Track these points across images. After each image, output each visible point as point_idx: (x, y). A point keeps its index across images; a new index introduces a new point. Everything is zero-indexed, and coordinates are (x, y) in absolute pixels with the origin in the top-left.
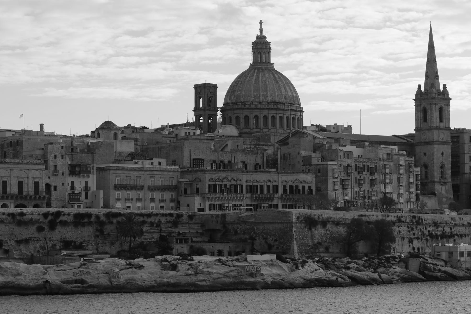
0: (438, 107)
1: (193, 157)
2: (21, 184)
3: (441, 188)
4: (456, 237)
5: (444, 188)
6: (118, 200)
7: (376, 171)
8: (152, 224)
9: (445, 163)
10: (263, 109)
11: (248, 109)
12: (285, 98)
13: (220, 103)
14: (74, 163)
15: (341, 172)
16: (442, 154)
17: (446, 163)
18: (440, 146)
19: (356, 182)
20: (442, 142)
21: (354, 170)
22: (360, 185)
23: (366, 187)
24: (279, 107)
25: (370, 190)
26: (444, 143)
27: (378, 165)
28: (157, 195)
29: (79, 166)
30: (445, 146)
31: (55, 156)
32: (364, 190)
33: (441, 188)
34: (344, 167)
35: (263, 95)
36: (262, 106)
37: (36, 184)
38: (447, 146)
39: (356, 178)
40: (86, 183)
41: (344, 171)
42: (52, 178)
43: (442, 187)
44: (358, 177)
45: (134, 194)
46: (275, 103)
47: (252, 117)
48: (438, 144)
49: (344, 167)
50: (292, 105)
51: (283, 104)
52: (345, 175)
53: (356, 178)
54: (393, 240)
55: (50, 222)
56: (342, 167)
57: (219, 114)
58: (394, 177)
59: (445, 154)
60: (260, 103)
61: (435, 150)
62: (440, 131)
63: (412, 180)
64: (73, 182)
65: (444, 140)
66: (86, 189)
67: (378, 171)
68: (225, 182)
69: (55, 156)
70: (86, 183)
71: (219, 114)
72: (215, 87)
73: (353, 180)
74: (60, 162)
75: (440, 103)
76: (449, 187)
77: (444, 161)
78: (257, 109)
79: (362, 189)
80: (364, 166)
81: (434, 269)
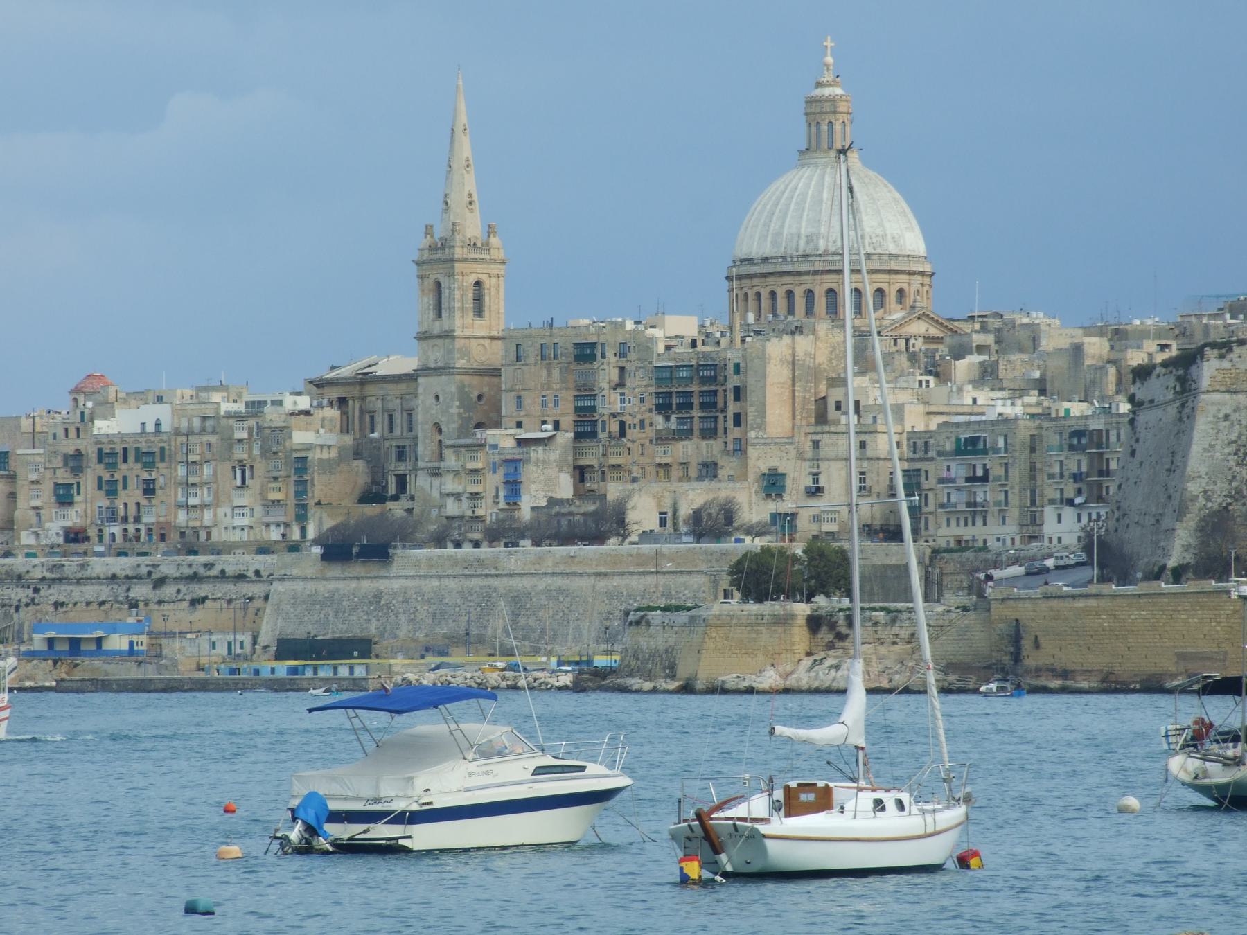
7: (162, 460)
9: (443, 420)
12: (775, 243)
15: (55, 469)
16: (437, 397)
18: (431, 379)
19: (100, 488)
20: (435, 369)
21: (95, 460)
22: (112, 492)
23: (131, 496)
25: (144, 502)
27: (169, 445)
34: (66, 458)
38: (447, 377)
41: (66, 464)
44: (107, 477)
46: (751, 261)
47: (781, 293)
52: (68, 475)
53: (100, 478)
56: (60, 458)
61: (420, 390)
62: (431, 342)
65: (439, 364)
67: (167, 459)
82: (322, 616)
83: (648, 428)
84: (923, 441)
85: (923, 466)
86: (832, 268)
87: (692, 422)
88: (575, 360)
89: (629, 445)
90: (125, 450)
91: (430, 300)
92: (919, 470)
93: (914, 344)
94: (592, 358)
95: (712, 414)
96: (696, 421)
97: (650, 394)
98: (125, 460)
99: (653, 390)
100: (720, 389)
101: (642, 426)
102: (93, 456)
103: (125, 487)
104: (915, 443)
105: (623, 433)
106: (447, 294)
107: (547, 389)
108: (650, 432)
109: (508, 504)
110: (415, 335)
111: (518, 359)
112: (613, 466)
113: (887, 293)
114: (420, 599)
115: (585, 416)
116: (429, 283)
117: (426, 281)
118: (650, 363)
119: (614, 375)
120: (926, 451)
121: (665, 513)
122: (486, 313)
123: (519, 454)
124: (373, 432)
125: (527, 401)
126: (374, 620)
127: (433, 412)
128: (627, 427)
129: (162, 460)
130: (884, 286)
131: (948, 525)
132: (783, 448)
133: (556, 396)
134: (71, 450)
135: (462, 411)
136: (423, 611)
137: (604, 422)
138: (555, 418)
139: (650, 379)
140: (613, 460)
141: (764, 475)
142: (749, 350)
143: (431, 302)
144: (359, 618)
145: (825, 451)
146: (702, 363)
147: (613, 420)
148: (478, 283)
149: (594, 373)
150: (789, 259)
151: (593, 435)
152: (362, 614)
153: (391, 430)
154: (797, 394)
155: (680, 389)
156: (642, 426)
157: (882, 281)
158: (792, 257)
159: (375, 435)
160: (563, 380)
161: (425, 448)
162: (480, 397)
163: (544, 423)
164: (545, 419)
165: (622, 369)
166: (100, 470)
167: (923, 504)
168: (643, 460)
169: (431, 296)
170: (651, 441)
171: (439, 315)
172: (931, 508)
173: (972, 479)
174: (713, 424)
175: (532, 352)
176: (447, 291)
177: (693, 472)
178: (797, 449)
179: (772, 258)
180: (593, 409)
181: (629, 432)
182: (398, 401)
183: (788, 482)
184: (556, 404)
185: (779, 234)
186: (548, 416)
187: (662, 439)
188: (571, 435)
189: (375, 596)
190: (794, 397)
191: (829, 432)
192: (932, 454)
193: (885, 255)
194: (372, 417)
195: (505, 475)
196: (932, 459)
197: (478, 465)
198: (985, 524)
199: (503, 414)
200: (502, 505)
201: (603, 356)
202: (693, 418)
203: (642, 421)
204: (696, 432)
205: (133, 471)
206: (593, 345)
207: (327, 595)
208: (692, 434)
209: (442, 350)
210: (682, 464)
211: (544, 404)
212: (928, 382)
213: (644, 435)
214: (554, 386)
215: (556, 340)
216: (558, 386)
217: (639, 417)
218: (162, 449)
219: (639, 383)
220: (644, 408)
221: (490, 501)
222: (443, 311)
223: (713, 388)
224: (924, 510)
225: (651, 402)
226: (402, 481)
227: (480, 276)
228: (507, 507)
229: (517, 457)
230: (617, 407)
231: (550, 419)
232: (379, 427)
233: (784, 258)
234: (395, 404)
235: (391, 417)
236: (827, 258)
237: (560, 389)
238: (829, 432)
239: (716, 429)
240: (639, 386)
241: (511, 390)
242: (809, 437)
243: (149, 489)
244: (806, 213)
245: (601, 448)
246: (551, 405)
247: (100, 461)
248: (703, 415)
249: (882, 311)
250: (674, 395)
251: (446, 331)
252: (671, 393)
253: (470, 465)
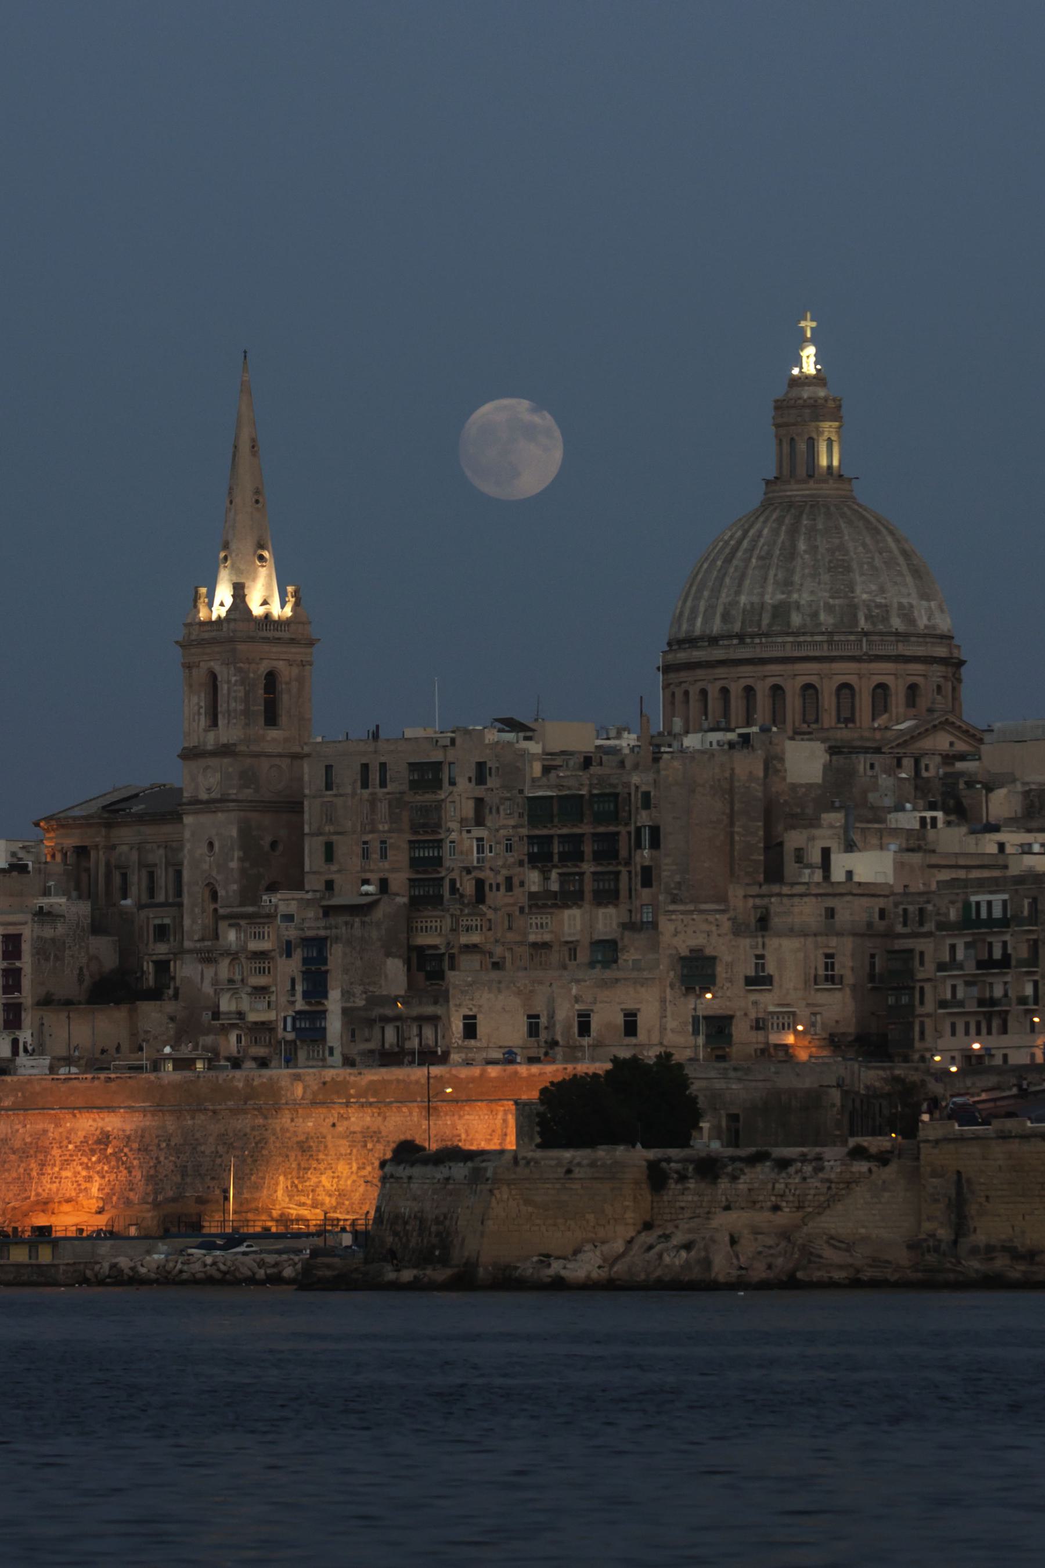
3: (202, 971)
5: (209, 972)
12: (726, 617)
16: (211, 845)
17: (219, 878)
18: (205, 819)
30: (220, 814)
33: (202, 971)
43: (205, 970)
48: (196, 813)
50: (748, 640)
51: (713, 641)
61: (187, 835)
65: (213, 795)
75: (206, 658)
77: (214, 873)
82: (21, 1170)
83: (517, 890)
84: (917, 907)
86: (811, 654)
87: (581, 881)
88: (411, 788)
89: (490, 914)
91: (199, 700)
92: (911, 951)
93: (927, 769)
94: (436, 784)
95: (611, 868)
96: (588, 879)
97: (521, 838)
99: (524, 831)
100: (621, 829)
101: (509, 888)
104: (905, 910)
105: (480, 896)
106: (225, 691)
107: (372, 832)
108: (519, 896)
109: (309, 1003)
110: (179, 751)
111: (329, 786)
112: (467, 946)
113: (893, 691)
114: (164, 1145)
115: (425, 872)
116: (200, 675)
117: (195, 671)
118: (521, 791)
119: (468, 809)
120: (921, 923)
121: (537, 1017)
122: (283, 720)
123: (325, 928)
124: (125, 898)
125: (340, 851)
126: (97, 1178)
127: (206, 867)
128: (487, 888)
130: (889, 680)
131: (953, 1033)
132: (711, 918)
133: (383, 842)
135: (247, 865)
137: (453, 882)
138: (382, 875)
139: (521, 815)
140: (464, 939)
141: (682, 959)
142: (663, 773)
143: (202, 704)
144: (76, 1174)
145: (776, 921)
146: (595, 792)
147: (467, 878)
148: (271, 677)
149: (439, 806)
150: (748, 640)
151: (437, 901)
152: (80, 1168)
153: (151, 892)
154: (737, 838)
155: (565, 831)
156: (509, 888)
157: (883, 672)
158: (752, 636)
159: (128, 902)
161: (194, 922)
162: (274, 845)
163: (366, 882)
164: (368, 876)
165: (479, 802)
167: (917, 1002)
168: (510, 936)
169: (203, 695)
170: (522, 910)
171: (215, 724)
172: (929, 1007)
173: (986, 964)
174: (612, 884)
175: (347, 777)
176: (225, 686)
177: (583, 956)
178: (733, 920)
179: (723, 637)
180: (438, 861)
181: (490, 896)
182: (161, 851)
183: (720, 969)
184: (384, 855)
185: (734, 603)
186: (372, 871)
187: (541, 902)
188: (403, 900)
189: (99, 1142)
190: (732, 843)
191: (779, 895)
192: (929, 926)
193: (890, 634)
194: (124, 876)
195: (306, 961)
196: (929, 934)
197: (265, 945)
199: (307, 868)
201: (453, 783)
202: (582, 874)
203: (509, 880)
204: (588, 895)
206: (437, 766)
207: (28, 1140)
208: (582, 899)
209: (218, 775)
210: (567, 942)
211: (366, 855)
212: (934, 820)
213: (511, 900)
214: (381, 827)
215: (383, 759)
216: (386, 828)
217: (505, 872)
220: (511, 860)
221: (283, 1000)
222: (220, 716)
223: (612, 829)
224: (919, 1010)
225: (522, 850)
226: (162, 967)
227: (275, 663)
228: (306, 1008)
229: (322, 933)
231: (374, 877)
232: (134, 890)
233: (741, 637)
234: (157, 856)
235: (151, 875)
236: (801, 639)
237: (389, 831)
238: (779, 895)
239: (617, 892)
240: (505, 827)
241: (319, 833)
242: (751, 902)
244: (772, 573)
245: (449, 920)
246: (376, 856)
248: (599, 869)
249: (885, 716)
250: (556, 841)
251: (224, 745)
252: (551, 837)
253: (254, 946)
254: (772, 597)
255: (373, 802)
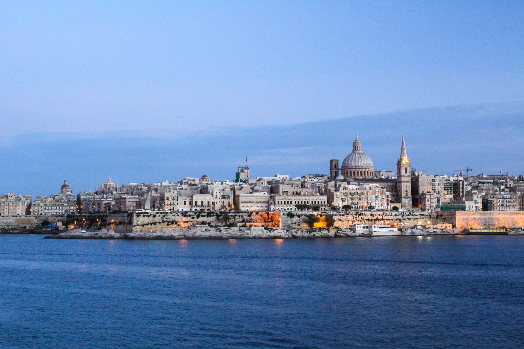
0: (404, 167)
1: (283, 191)
2: (202, 202)
4: (385, 220)
5: (407, 200)
6: (243, 207)
7: (362, 194)
8: (239, 216)
10: (353, 169)
11: (347, 169)
12: (364, 164)
13: (340, 166)
14: (224, 194)
16: (406, 186)
19: (350, 199)
24: (360, 168)
25: (359, 202)
26: (407, 182)
28: (260, 205)
29: (226, 195)
31: (216, 192)
32: (355, 202)
34: (343, 193)
35: (354, 163)
36: (353, 168)
37: (208, 202)
39: (350, 197)
40: (229, 201)
41: (343, 195)
42: (215, 200)
44: (352, 197)
45: (250, 205)
46: (359, 166)
49: (343, 193)
51: (363, 166)
53: (350, 197)
54: (334, 221)
55: (197, 215)
57: (340, 171)
58: (374, 197)
59: (407, 186)
60: (352, 166)
63: (383, 197)
64: (223, 201)
66: (229, 203)
68: (285, 200)
69: (216, 192)
70: (229, 201)
71: (340, 171)
72: (338, 161)
73: (349, 198)
74: (218, 194)
76: (410, 199)
78: (350, 169)
79: (354, 201)
80: (355, 193)
81: (342, 233)
85: (493, 200)
90: (355, 193)
98: (355, 194)
99: (443, 187)
102: (349, 194)
103: (355, 199)
119: (438, 184)
129: (362, 194)
134: (344, 192)
136: (483, 221)
160: (430, 185)
165: (439, 183)
166: (350, 196)
198: (509, 208)
200: (437, 204)
205: (356, 196)
206: (435, 179)
218: (362, 193)
219: (442, 186)
225: (443, 189)
230: (438, 189)
243: (360, 199)
247: (350, 194)
254: (369, 163)
255: (428, 183)
